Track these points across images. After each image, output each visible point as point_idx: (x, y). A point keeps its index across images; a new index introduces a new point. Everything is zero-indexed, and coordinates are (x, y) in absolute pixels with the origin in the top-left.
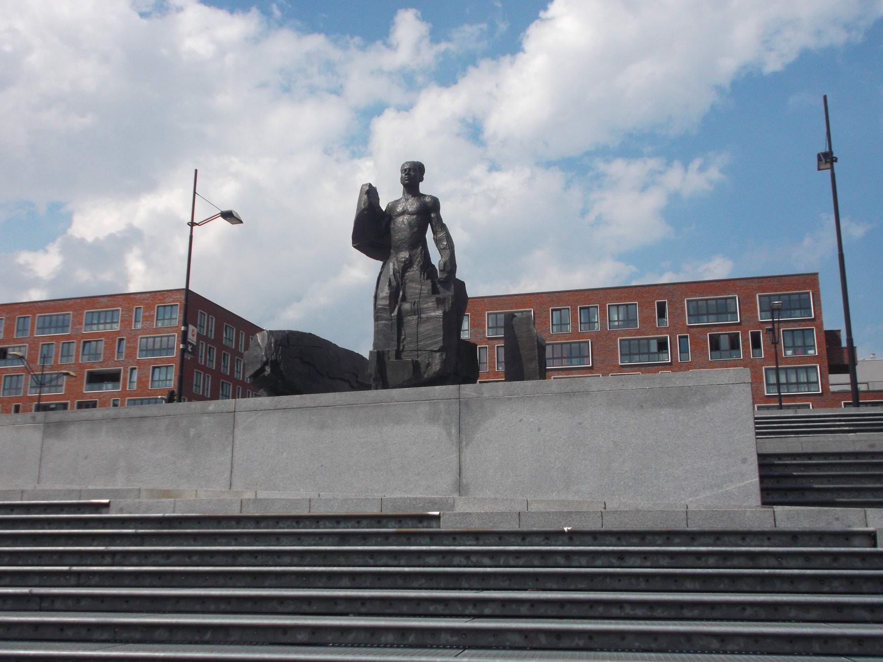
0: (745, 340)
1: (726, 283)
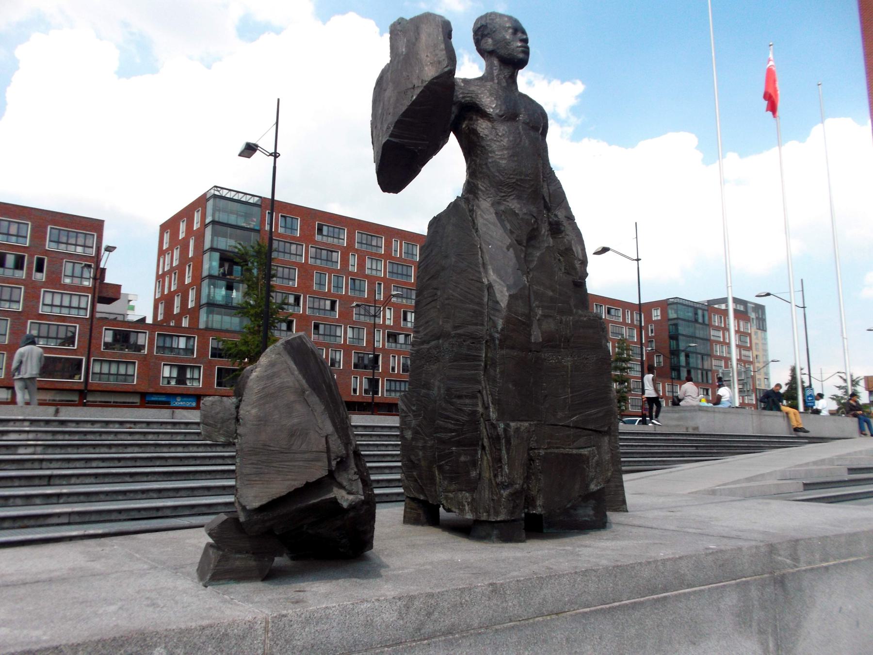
0: (30, 263)
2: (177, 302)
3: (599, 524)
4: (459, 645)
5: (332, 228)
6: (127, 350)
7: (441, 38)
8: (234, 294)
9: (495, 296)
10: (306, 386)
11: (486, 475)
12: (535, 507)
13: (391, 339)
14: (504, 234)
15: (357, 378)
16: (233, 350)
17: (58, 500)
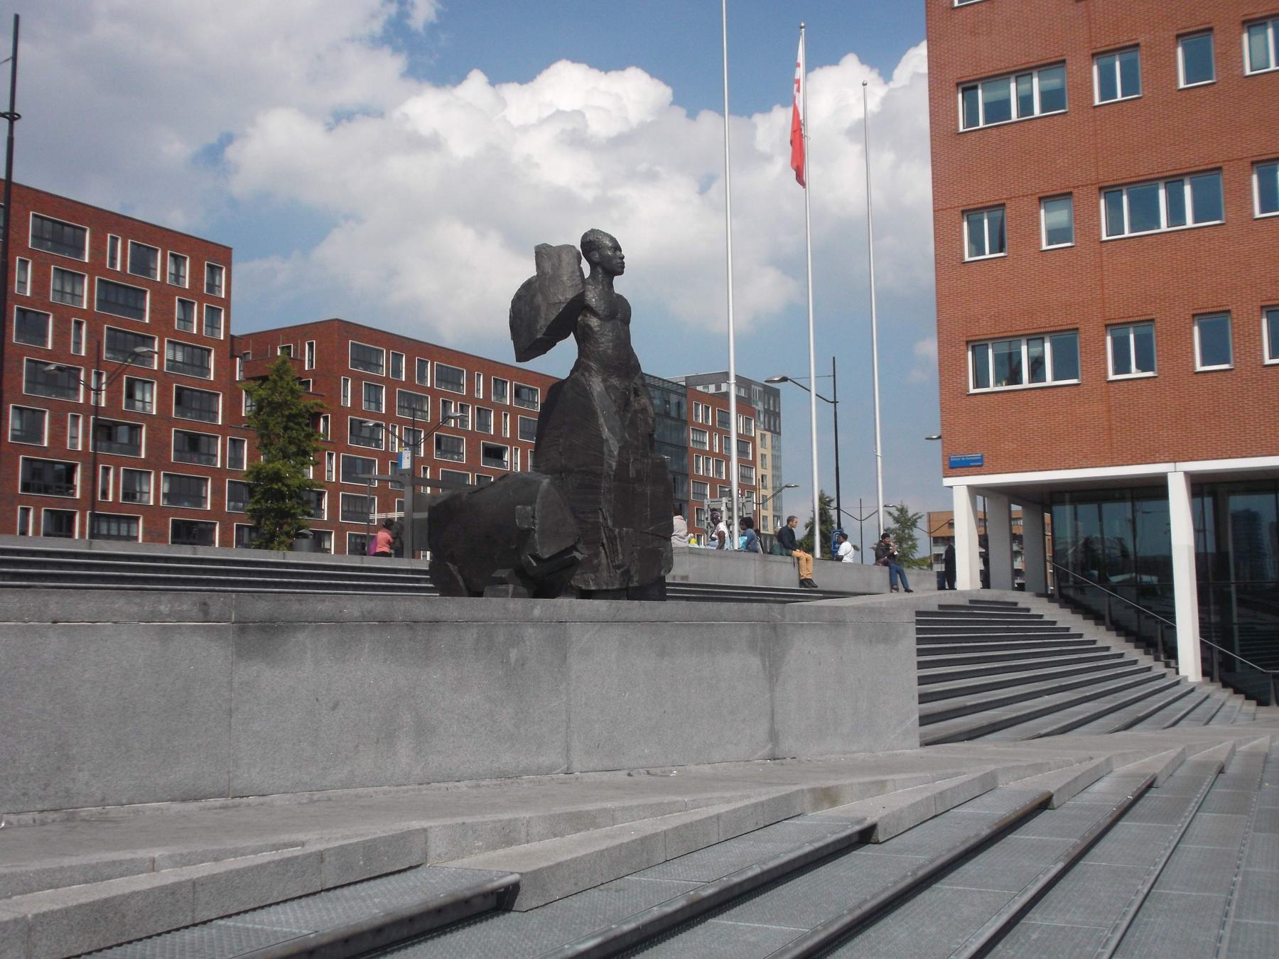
11: (604, 561)
13: (99, 434)
15: (27, 510)
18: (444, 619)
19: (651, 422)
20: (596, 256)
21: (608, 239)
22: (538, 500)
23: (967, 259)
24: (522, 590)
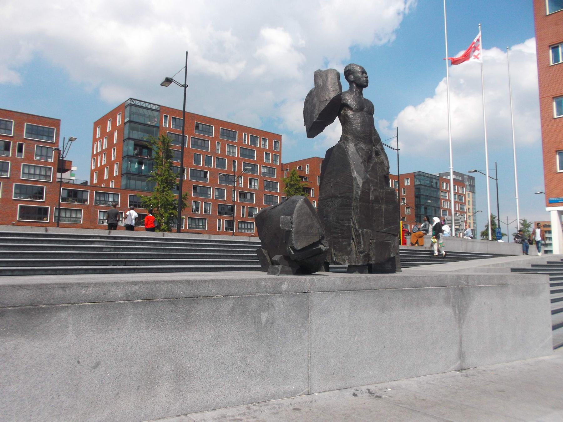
1: (7, 112)
2: (106, 171)
3: (393, 271)
4: (357, 294)
5: (205, 126)
6: (76, 202)
7: (336, 80)
8: (143, 167)
9: (357, 182)
10: (311, 213)
11: (354, 249)
12: (371, 261)
13: (241, 196)
14: (359, 158)
16: (148, 202)
17: (134, 271)
18: (204, 295)
19: (386, 169)
20: (352, 77)
21: (359, 68)
22: (295, 212)
23: (555, 116)
24: (288, 268)
